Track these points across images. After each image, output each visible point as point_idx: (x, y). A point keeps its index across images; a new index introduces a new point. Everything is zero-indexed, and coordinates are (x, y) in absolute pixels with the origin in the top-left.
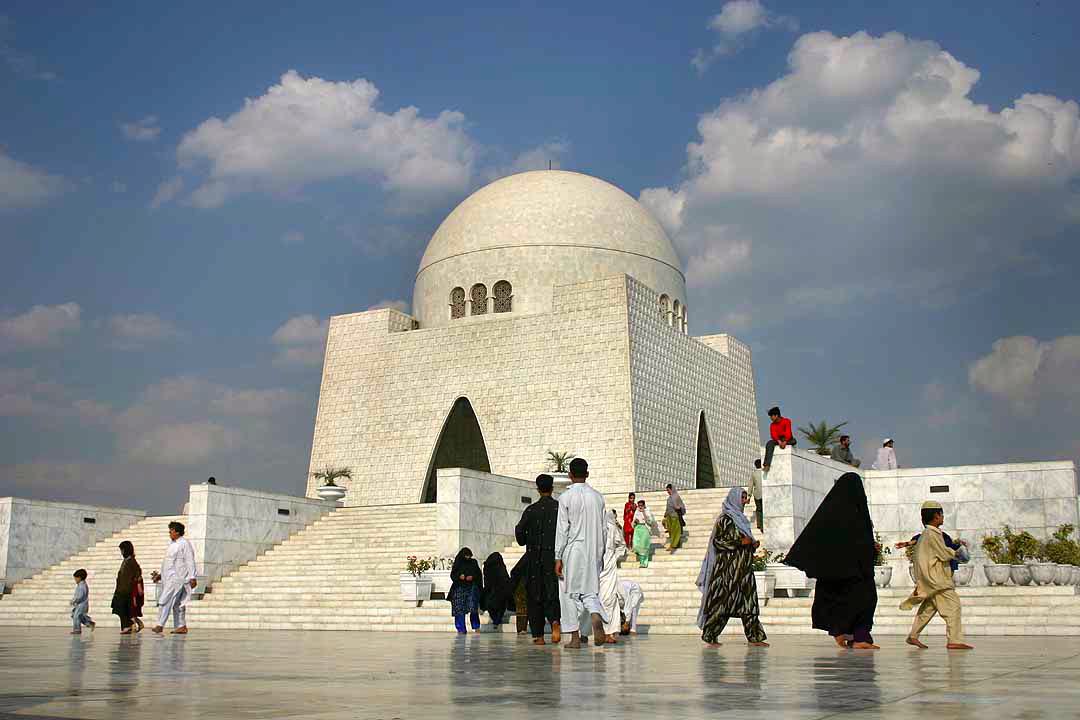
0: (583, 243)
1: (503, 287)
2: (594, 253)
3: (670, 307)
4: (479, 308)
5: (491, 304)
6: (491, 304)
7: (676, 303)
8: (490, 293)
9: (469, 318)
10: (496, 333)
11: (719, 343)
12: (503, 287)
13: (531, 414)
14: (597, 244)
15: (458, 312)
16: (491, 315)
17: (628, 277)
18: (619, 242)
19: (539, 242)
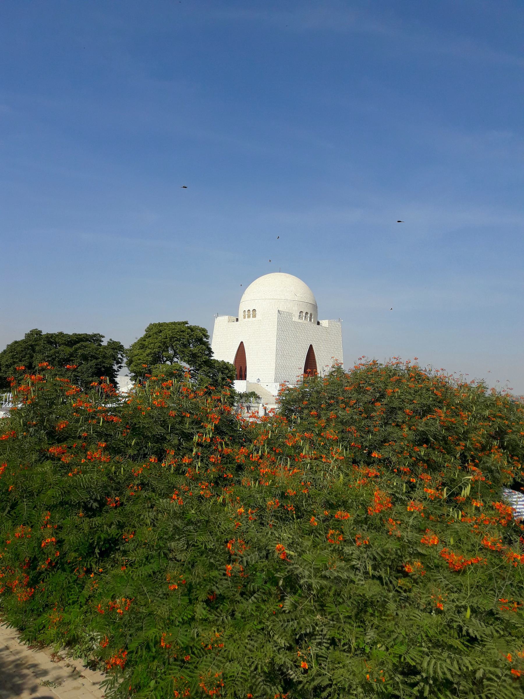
3: (304, 314)
4: (249, 317)
5: (251, 315)
6: (251, 315)
7: (307, 313)
8: (251, 313)
9: (247, 319)
15: (244, 318)
16: (251, 319)
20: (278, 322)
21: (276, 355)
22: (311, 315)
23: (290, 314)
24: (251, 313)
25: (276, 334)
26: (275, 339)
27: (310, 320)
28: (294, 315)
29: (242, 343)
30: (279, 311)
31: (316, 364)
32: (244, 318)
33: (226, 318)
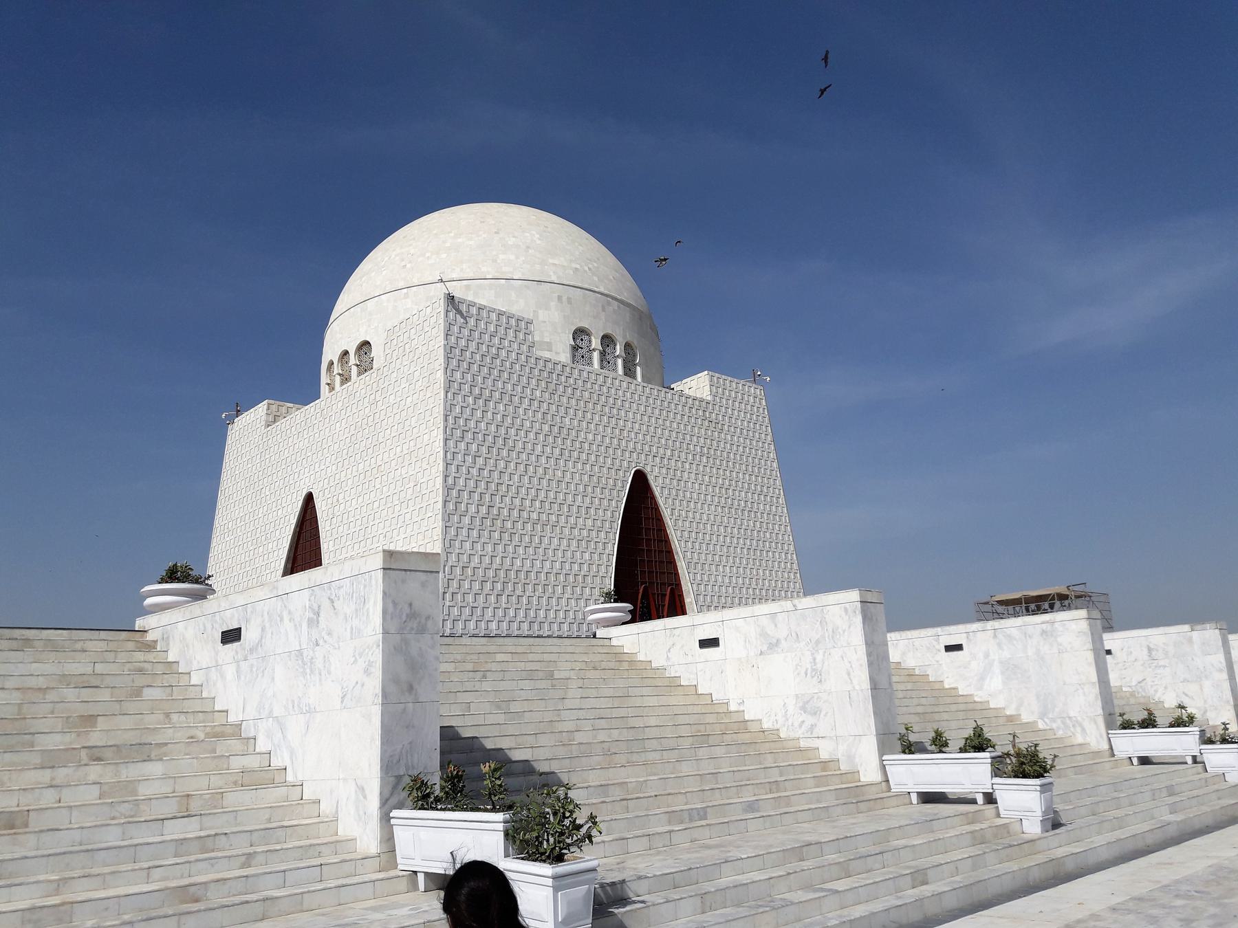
0: (455, 276)
1: (365, 345)
2: (468, 287)
3: (596, 343)
4: (345, 379)
6: (354, 370)
7: (607, 340)
10: (340, 404)
11: (698, 385)
12: (365, 345)
13: (360, 499)
14: (471, 275)
15: (332, 389)
17: (451, 299)
18: (505, 269)
19: (401, 285)
20: (449, 351)
21: (447, 517)
22: (628, 346)
23: (521, 326)
24: (353, 359)
25: (439, 411)
26: (435, 438)
27: (629, 372)
28: (549, 346)
29: (309, 498)
30: (451, 299)
31: (672, 563)
32: (332, 389)
33: (262, 408)
